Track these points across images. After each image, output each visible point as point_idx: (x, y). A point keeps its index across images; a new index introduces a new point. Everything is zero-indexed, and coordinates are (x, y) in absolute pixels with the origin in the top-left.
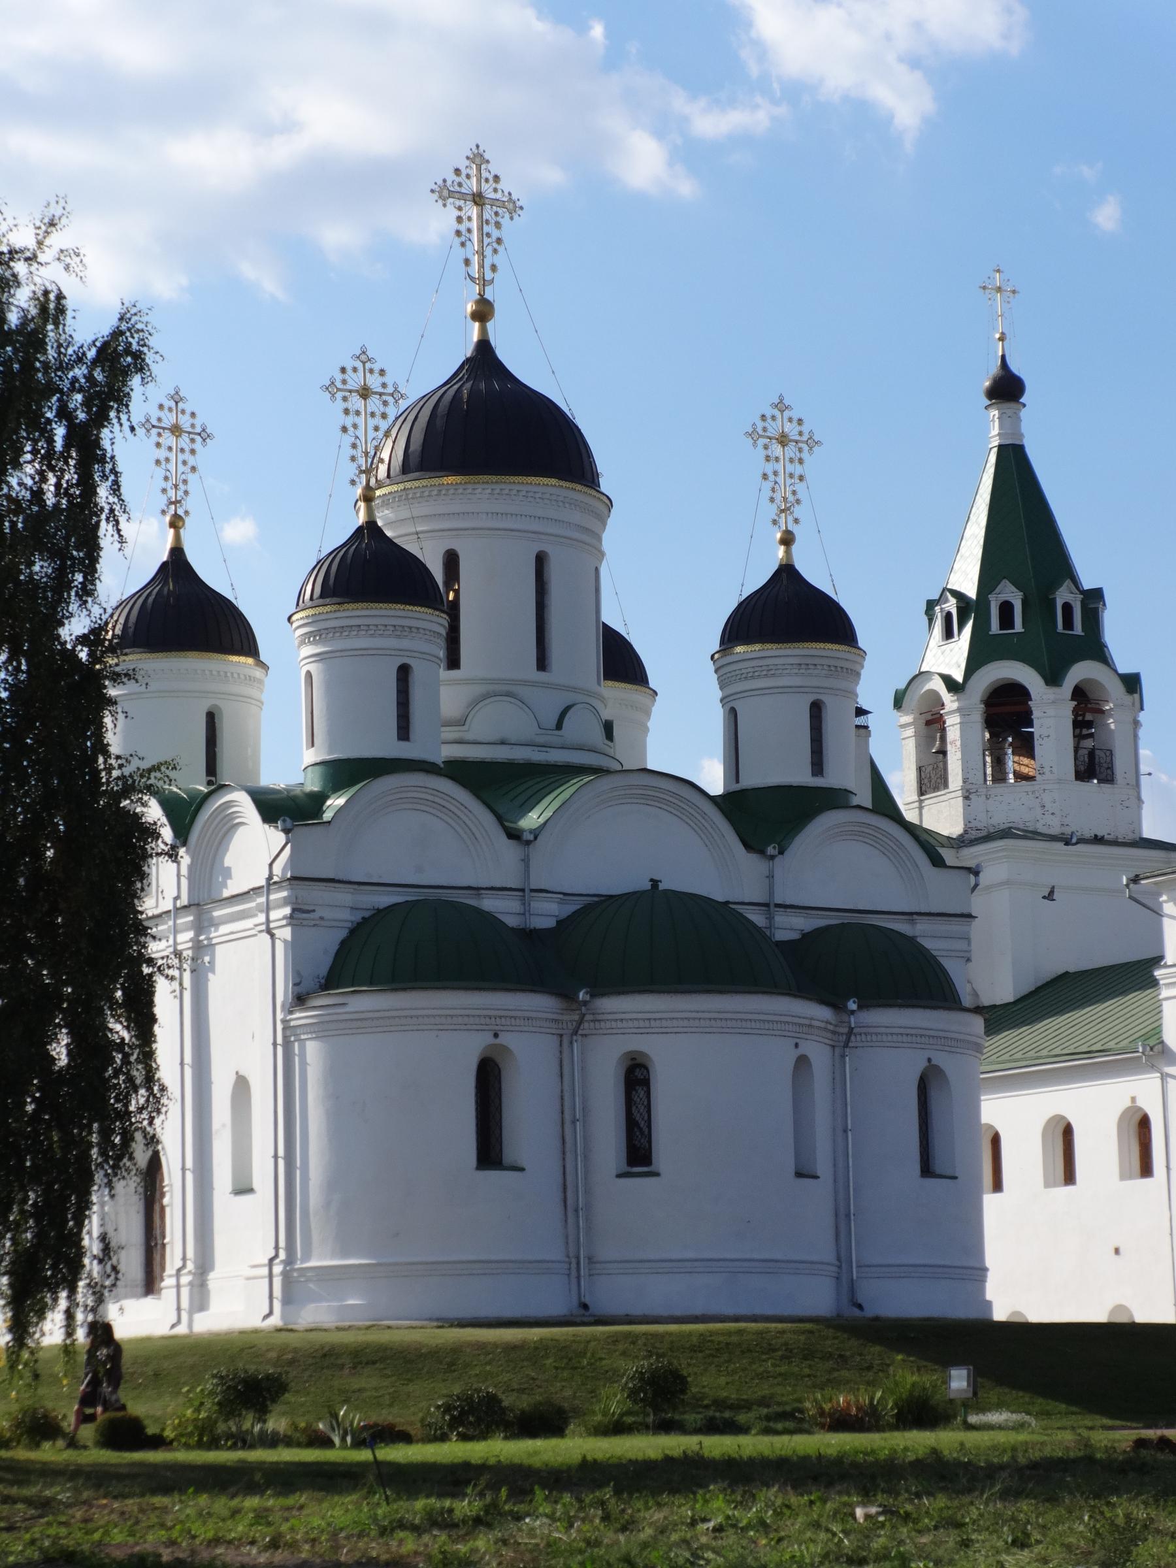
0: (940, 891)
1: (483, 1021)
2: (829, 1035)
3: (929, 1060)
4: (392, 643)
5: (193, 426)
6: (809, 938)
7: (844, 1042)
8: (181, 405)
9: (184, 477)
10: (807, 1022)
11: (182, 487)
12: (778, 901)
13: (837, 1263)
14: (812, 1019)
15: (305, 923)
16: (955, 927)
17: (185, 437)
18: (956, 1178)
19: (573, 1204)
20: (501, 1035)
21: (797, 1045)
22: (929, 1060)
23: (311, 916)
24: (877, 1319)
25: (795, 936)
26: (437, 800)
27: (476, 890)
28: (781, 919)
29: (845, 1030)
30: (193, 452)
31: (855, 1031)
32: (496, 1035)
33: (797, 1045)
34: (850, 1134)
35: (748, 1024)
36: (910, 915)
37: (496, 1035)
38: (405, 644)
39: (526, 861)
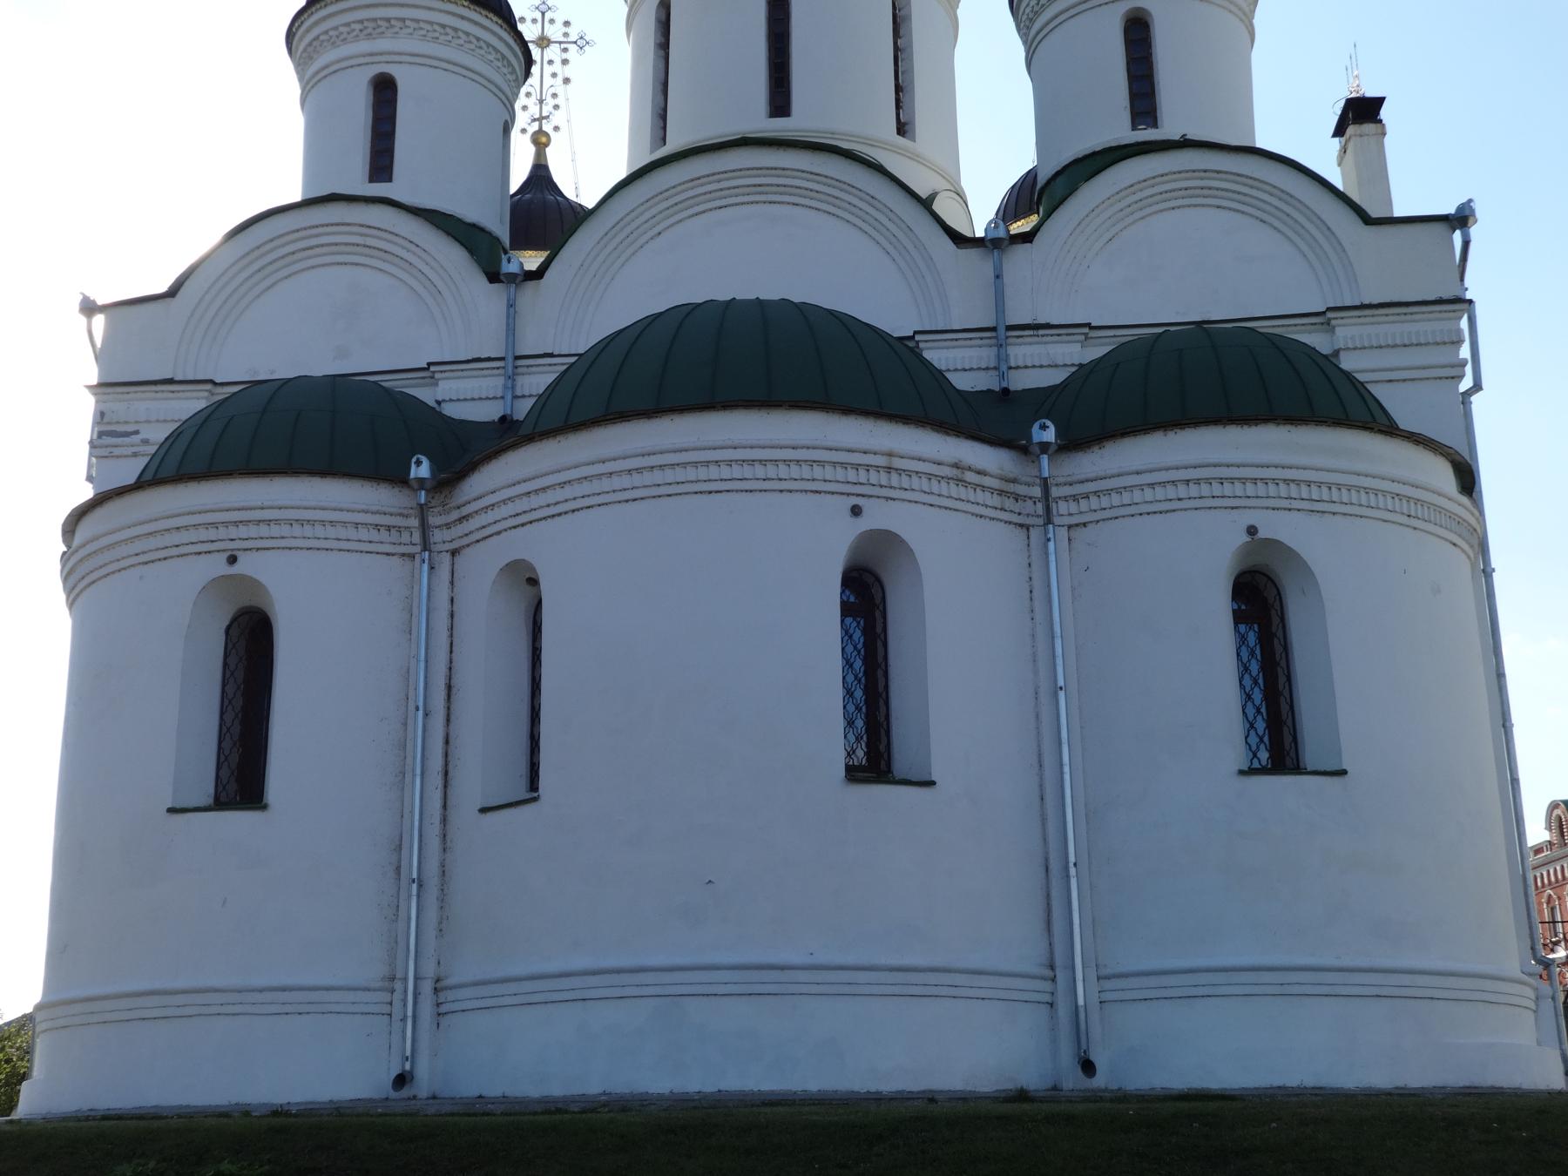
0: (1379, 269)
1: (203, 534)
2: (995, 500)
3: (1252, 531)
4: (364, 46)
5: (534, 21)
6: (1085, 373)
7: (1040, 514)
8: (548, 15)
9: (552, 90)
10: (881, 461)
11: (550, 102)
12: (1019, 313)
13: (1048, 973)
14: (890, 455)
15: (117, 451)
16: (1425, 326)
17: (555, 48)
18: (1344, 772)
19: (421, 877)
20: (241, 557)
21: (856, 511)
22: (1252, 531)
23: (136, 439)
24: (1122, 1097)
25: (1056, 377)
26: (370, 242)
27: (429, 371)
28: (1022, 351)
29: (1037, 491)
30: (565, 62)
31: (1055, 492)
32: (232, 560)
33: (856, 511)
34: (1062, 694)
35: (714, 472)
36: (1324, 318)
37: (232, 560)
38: (383, 44)
39: (511, 305)
